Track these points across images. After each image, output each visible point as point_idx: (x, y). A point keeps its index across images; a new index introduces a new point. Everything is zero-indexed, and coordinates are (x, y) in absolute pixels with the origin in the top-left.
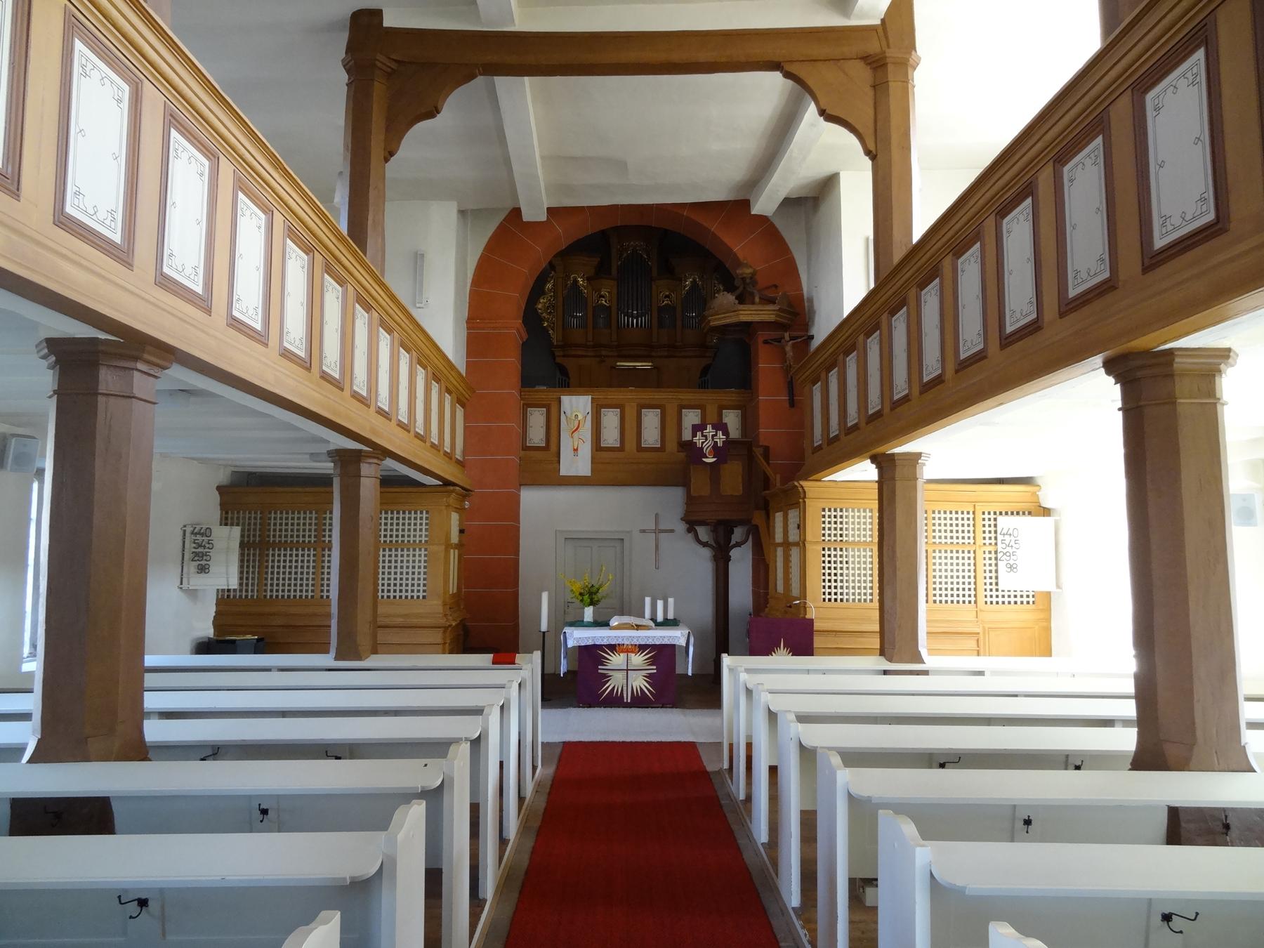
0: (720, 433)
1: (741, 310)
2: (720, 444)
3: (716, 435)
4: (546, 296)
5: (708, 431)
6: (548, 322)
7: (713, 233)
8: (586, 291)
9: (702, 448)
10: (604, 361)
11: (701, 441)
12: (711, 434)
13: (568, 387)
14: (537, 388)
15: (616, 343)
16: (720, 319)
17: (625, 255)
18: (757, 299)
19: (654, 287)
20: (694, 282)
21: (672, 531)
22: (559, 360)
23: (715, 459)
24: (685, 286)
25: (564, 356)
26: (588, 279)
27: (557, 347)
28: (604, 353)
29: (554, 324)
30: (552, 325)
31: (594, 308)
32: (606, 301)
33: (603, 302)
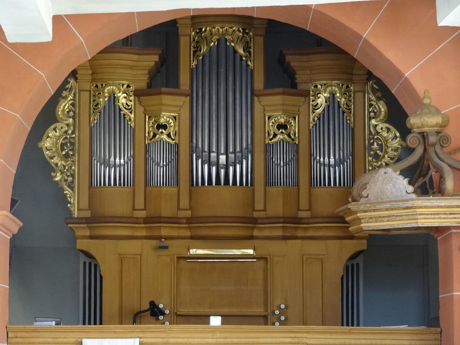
1: (420, 207)
4: (59, 125)
6: (62, 173)
7: (366, 41)
10: (166, 248)
13: (101, 324)
14: (38, 324)
15: (188, 214)
16: (377, 219)
17: (204, 49)
18: (449, 184)
19: (257, 105)
20: (332, 98)
22: (82, 244)
24: (316, 107)
25: (91, 237)
26: (138, 94)
27: (79, 220)
28: (164, 232)
29: (73, 176)
30: (70, 179)
32: (169, 135)
33: (164, 137)
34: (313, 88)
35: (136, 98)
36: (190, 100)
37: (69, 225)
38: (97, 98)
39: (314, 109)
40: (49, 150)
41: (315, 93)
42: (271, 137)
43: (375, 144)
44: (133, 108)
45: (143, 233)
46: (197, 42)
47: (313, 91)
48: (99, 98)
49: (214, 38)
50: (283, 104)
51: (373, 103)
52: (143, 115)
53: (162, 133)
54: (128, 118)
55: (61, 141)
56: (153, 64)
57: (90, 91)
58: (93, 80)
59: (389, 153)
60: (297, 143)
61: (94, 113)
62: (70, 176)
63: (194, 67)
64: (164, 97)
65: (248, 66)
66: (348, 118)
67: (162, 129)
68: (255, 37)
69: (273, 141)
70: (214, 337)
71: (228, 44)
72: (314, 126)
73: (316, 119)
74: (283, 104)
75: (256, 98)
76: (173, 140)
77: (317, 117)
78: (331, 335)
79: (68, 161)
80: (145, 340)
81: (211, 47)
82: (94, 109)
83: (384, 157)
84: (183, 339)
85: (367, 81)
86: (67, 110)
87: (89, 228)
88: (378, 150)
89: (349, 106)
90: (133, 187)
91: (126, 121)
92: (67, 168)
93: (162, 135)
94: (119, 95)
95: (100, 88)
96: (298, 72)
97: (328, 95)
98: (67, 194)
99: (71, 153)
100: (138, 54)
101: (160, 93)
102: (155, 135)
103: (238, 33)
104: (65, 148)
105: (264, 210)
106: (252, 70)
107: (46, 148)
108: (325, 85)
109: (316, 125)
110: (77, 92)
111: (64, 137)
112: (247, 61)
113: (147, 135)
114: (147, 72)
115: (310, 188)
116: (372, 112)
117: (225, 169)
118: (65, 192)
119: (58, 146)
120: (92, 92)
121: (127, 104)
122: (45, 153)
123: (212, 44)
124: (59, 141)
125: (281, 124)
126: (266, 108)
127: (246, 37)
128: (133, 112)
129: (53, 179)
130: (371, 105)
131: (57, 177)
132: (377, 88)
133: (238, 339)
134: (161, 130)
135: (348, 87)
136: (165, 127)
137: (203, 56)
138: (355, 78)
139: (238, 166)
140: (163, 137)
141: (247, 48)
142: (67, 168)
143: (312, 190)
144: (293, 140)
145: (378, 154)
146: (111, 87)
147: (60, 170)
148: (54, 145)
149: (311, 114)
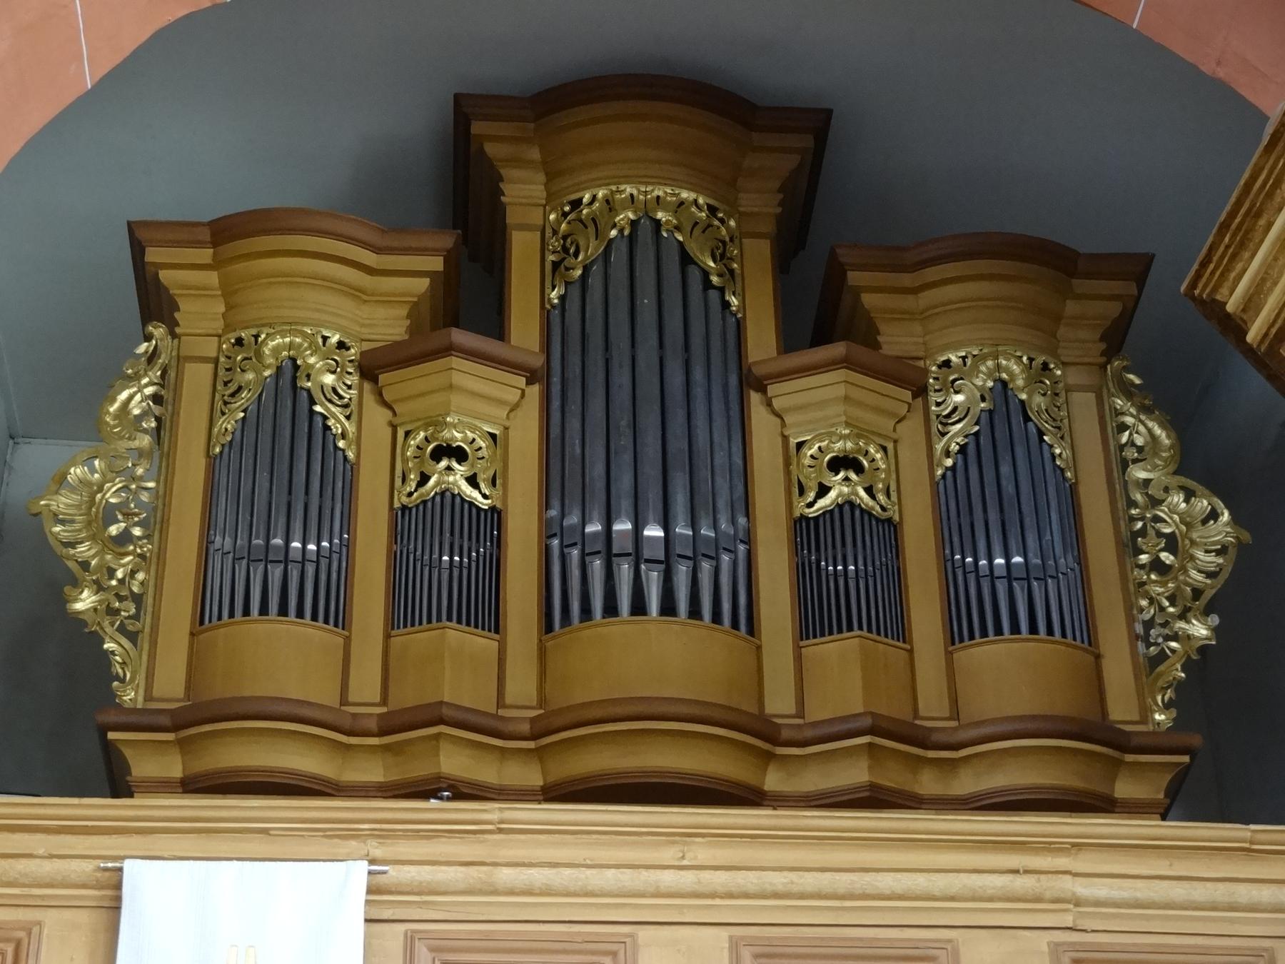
6: (99, 587)
8: (351, 428)
26: (370, 369)
31: (401, 518)
32: (472, 481)
34: (934, 368)
35: (367, 386)
36: (541, 392)
37: (112, 735)
38: (239, 370)
39: (945, 425)
40: (63, 522)
41: (945, 380)
42: (811, 496)
43: (1151, 532)
44: (353, 406)
45: (373, 772)
46: (565, 238)
47: (935, 379)
48: (243, 371)
49: (621, 217)
50: (847, 399)
51: (1129, 420)
52: (389, 431)
53: (449, 468)
54: (337, 428)
55: (108, 495)
56: (424, 284)
57: (216, 361)
58: (228, 327)
59: (1198, 559)
60: (896, 518)
61: (225, 417)
62: (130, 599)
63: (556, 301)
64: (455, 361)
65: (726, 305)
66: (1058, 451)
67: (449, 457)
69: (817, 506)
70: (685, 862)
71: (665, 235)
72: (949, 473)
73: (954, 448)
74: (847, 399)
75: (755, 397)
76: (485, 496)
77: (958, 444)
78: (1171, 865)
79: (127, 554)
80: (395, 874)
81: (611, 241)
82: (226, 403)
84: (554, 871)
85: (1103, 359)
86: (136, 412)
87: (183, 745)
89: (1054, 420)
90: (346, 633)
91: (332, 437)
92: (120, 574)
93: (448, 475)
94: (312, 360)
95: (250, 343)
96: (882, 327)
97: (990, 384)
98: (113, 653)
99: (137, 532)
100: (378, 250)
101: (448, 350)
102: (424, 479)
103: (694, 209)
104: (120, 517)
105: (800, 713)
106: (738, 321)
107: (55, 515)
108: (974, 356)
109: (953, 469)
110: (174, 363)
111: (120, 485)
112: (722, 290)
113: (398, 482)
114: (404, 311)
115: (951, 649)
116: (1129, 444)
117: (662, 573)
118: (106, 646)
119: (97, 512)
120: (222, 359)
121: (334, 390)
122: (47, 531)
123: (614, 233)
124: (99, 496)
126: (788, 419)
127: (719, 228)
128: (354, 417)
129: (68, 606)
130: (1123, 427)
131: (82, 600)
132: (1137, 381)
133: (785, 873)
134: (444, 463)
135: (1045, 366)
136: (460, 456)
137: (586, 269)
138: (1067, 354)
139: (706, 566)
140: (451, 479)
141: (723, 256)
142: (120, 574)
144: (883, 509)
145: (1163, 563)
146: (287, 340)
147: (96, 582)
148: (81, 509)
149: (935, 438)
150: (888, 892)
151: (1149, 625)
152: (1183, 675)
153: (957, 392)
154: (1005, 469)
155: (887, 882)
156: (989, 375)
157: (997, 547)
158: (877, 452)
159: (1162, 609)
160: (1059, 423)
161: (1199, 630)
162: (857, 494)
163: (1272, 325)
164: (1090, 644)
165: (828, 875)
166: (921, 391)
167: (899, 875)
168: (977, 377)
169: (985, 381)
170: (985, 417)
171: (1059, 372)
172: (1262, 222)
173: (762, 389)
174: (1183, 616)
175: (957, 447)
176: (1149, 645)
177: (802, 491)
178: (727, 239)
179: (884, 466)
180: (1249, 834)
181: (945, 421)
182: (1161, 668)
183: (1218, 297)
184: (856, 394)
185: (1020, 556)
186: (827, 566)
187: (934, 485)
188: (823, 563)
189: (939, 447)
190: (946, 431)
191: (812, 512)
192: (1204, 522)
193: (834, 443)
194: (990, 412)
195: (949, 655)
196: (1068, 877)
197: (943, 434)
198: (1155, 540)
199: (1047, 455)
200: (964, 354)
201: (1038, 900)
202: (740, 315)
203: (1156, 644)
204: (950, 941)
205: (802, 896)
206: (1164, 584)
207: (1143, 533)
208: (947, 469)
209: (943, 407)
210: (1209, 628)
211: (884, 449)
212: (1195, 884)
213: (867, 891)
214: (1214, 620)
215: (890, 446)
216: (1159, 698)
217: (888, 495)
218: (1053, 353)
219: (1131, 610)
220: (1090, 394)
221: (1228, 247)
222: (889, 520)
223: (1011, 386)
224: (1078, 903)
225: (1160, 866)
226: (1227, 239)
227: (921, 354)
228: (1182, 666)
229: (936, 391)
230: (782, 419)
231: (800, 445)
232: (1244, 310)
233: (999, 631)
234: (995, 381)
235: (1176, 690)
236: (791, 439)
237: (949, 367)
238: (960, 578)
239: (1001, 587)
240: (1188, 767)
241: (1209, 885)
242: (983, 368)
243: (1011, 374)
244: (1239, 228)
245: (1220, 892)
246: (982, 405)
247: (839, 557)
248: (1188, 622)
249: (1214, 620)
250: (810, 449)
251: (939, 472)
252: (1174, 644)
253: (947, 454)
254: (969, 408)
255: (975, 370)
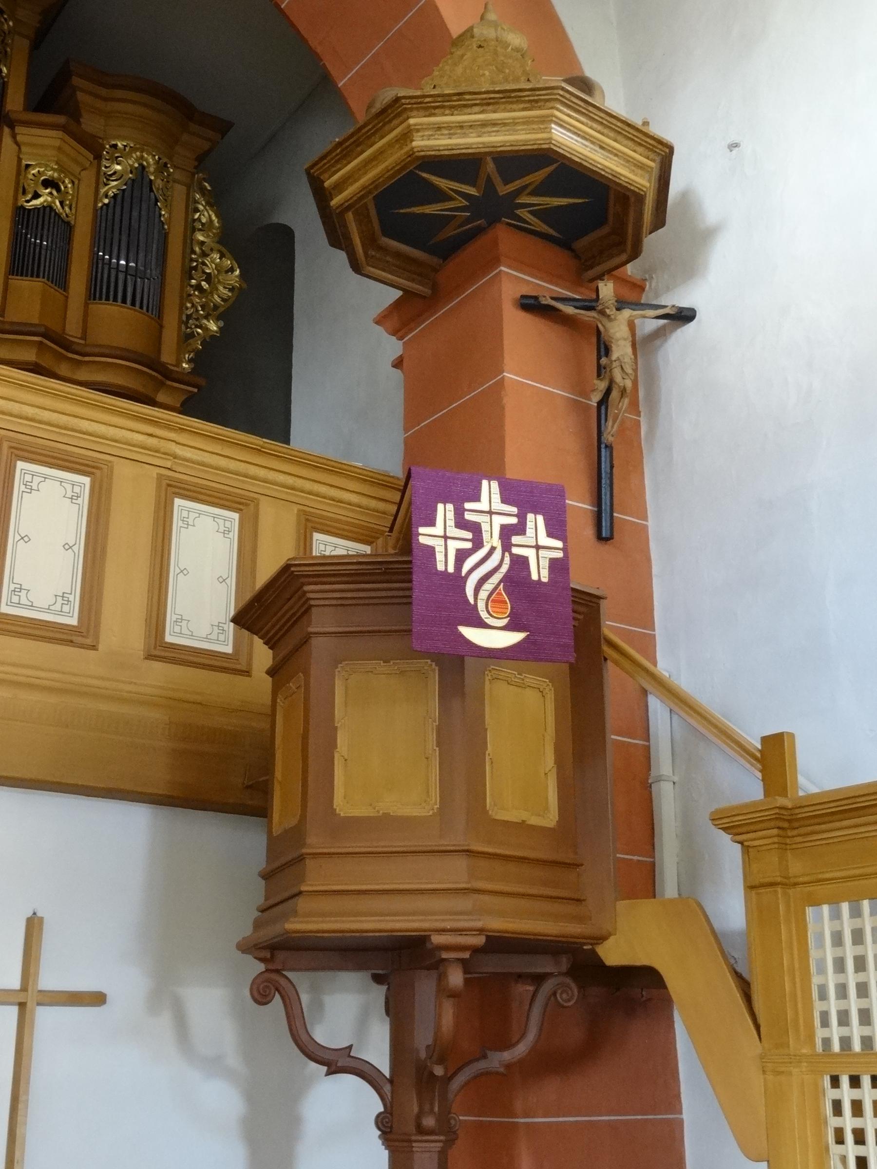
0: (536, 523)
2: (538, 571)
3: (520, 529)
5: (483, 505)
9: (457, 580)
11: (453, 546)
12: (498, 521)
21: (97, 999)
23: (514, 638)
34: (107, 146)
39: (108, 180)
42: (29, 197)
43: (200, 270)
50: (59, 149)
51: (201, 207)
60: (73, 222)
66: (163, 213)
68: (16, 37)
69: (31, 203)
73: (111, 194)
74: (59, 149)
77: (113, 192)
78: (222, 449)
83: (211, 293)
88: (203, 280)
89: (165, 195)
97: (136, 165)
108: (131, 147)
125: (50, 179)
126: (24, 149)
130: (196, 210)
132: (209, 188)
135: (165, 165)
143: (90, 306)
145: (202, 287)
149: (101, 185)
150: (85, 430)
151: (189, 317)
152: (201, 347)
153: (118, 164)
154: (135, 214)
155: (85, 425)
156: (137, 160)
157: (123, 253)
158: (69, 183)
159: (197, 311)
160: (166, 198)
161: (213, 326)
162: (55, 203)
163: (347, 201)
164: (159, 318)
165: (56, 414)
166: (98, 157)
167: (92, 423)
168: (131, 159)
169: (134, 163)
170: (130, 182)
171: (172, 170)
172: (359, 149)
173: (12, 127)
174: (206, 317)
175: (112, 194)
176: (187, 328)
177: (24, 192)
178: (7, 32)
179: (71, 192)
180: (262, 443)
181: (109, 177)
182: (191, 341)
183: (322, 177)
184: (67, 148)
185: (134, 263)
186: (31, 238)
187: (95, 209)
188: (29, 236)
189: (103, 191)
190: (108, 183)
191: (29, 205)
192: (227, 272)
193: (47, 171)
194: (133, 181)
195: (86, 305)
196: (174, 444)
197: (106, 185)
198: (201, 274)
199: (157, 213)
200: (125, 144)
201: (156, 451)
202: (6, 80)
203: (191, 328)
204: (110, 462)
205: (40, 422)
206: (200, 298)
207: (195, 268)
208: (105, 204)
209: (108, 169)
210: (218, 327)
211: (73, 183)
212: (232, 461)
213: (75, 428)
214: (221, 323)
215: (76, 182)
216: (187, 356)
217: (70, 209)
218: (170, 158)
219: (182, 307)
220: (184, 187)
221: (337, 155)
222: (68, 223)
223: (147, 170)
224: (175, 457)
225: (217, 448)
226: (338, 151)
227: (102, 136)
228: (201, 343)
229: (106, 159)
230: (20, 148)
231: (28, 166)
232: (333, 189)
233: (115, 300)
234: (139, 164)
235: (196, 355)
236: (23, 161)
237: (116, 149)
238: (100, 266)
239: (121, 276)
240: (194, 394)
241: (238, 463)
242: (134, 155)
243: (148, 163)
244: (347, 147)
245: (242, 467)
246: (131, 175)
247: (39, 235)
248: (209, 321)
249: (221, 323)
250: (33, 169)
251: (100, 205)
252: (199, 330)
253: (106, 196)
254: (122, 175)
255: (128, 156)
